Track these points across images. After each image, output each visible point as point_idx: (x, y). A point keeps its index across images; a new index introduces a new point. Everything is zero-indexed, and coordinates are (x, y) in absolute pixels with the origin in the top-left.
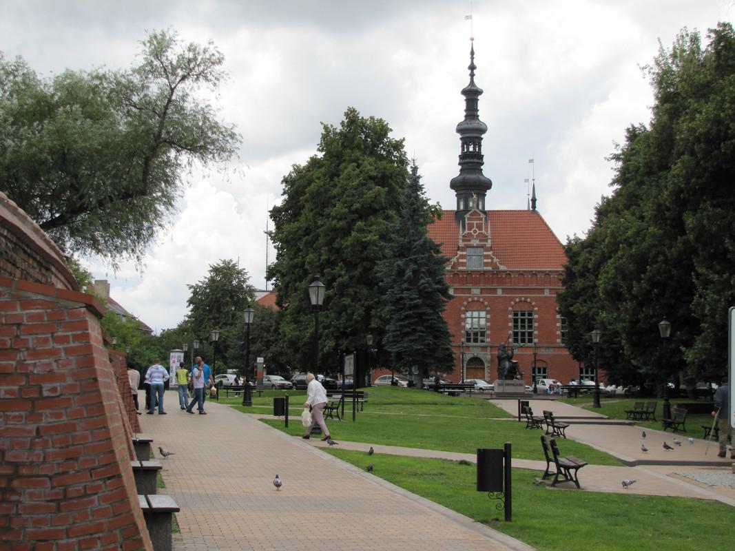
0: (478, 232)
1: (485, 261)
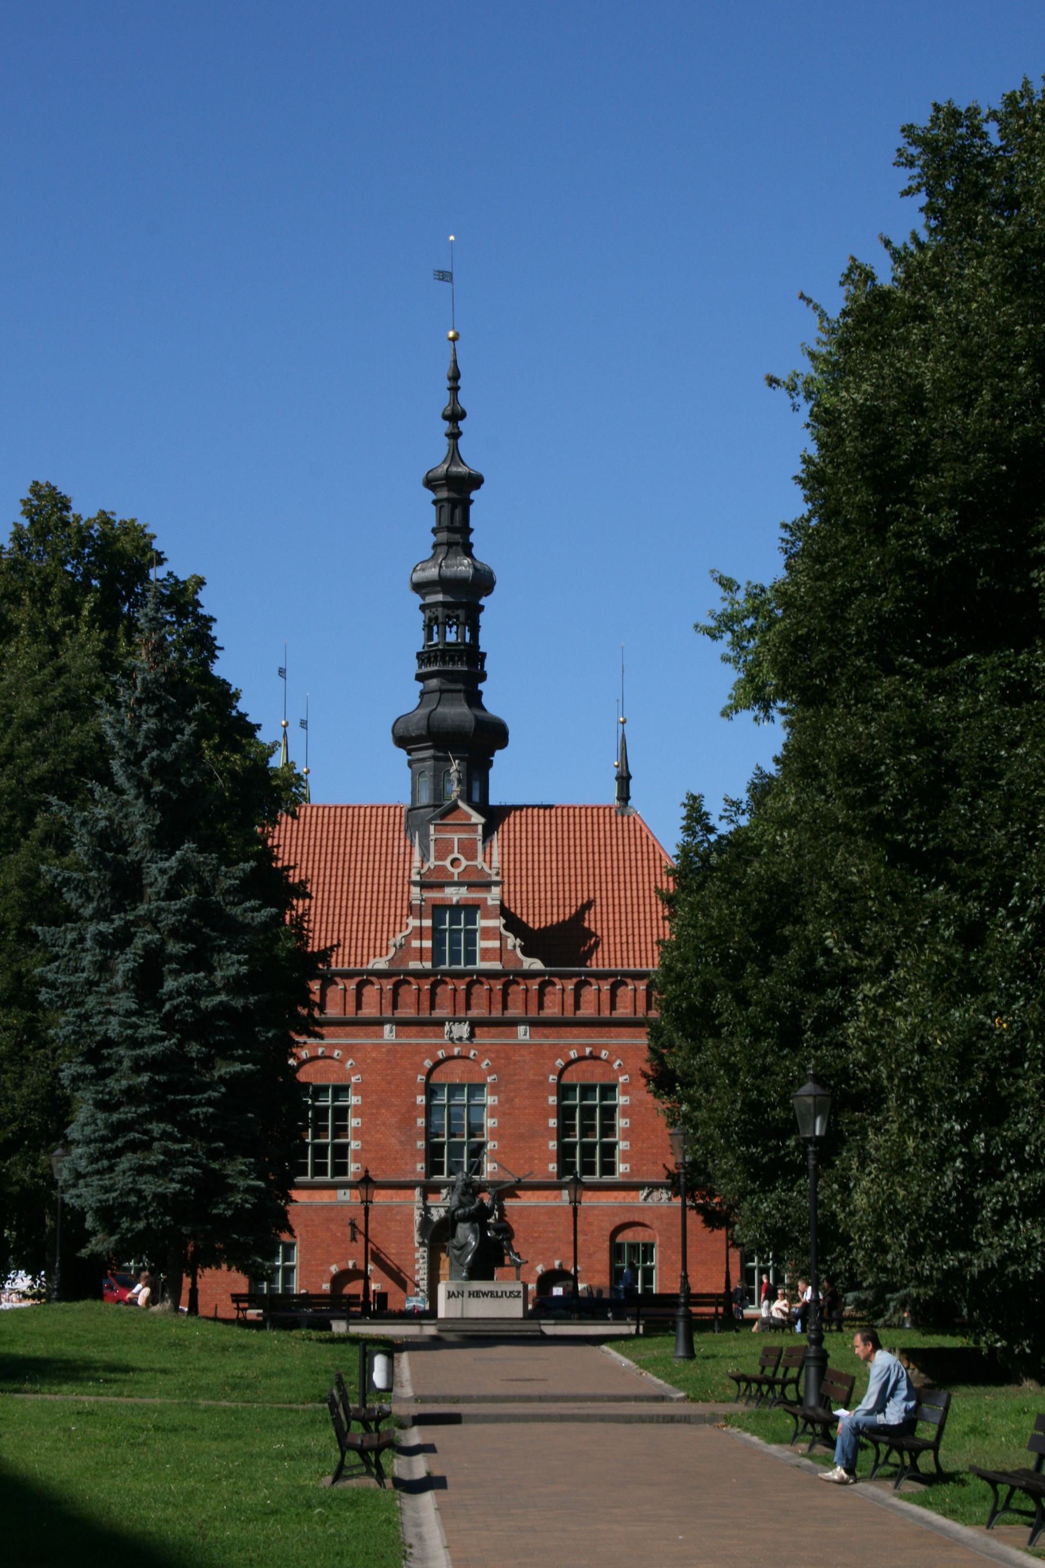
0: (464, 863)
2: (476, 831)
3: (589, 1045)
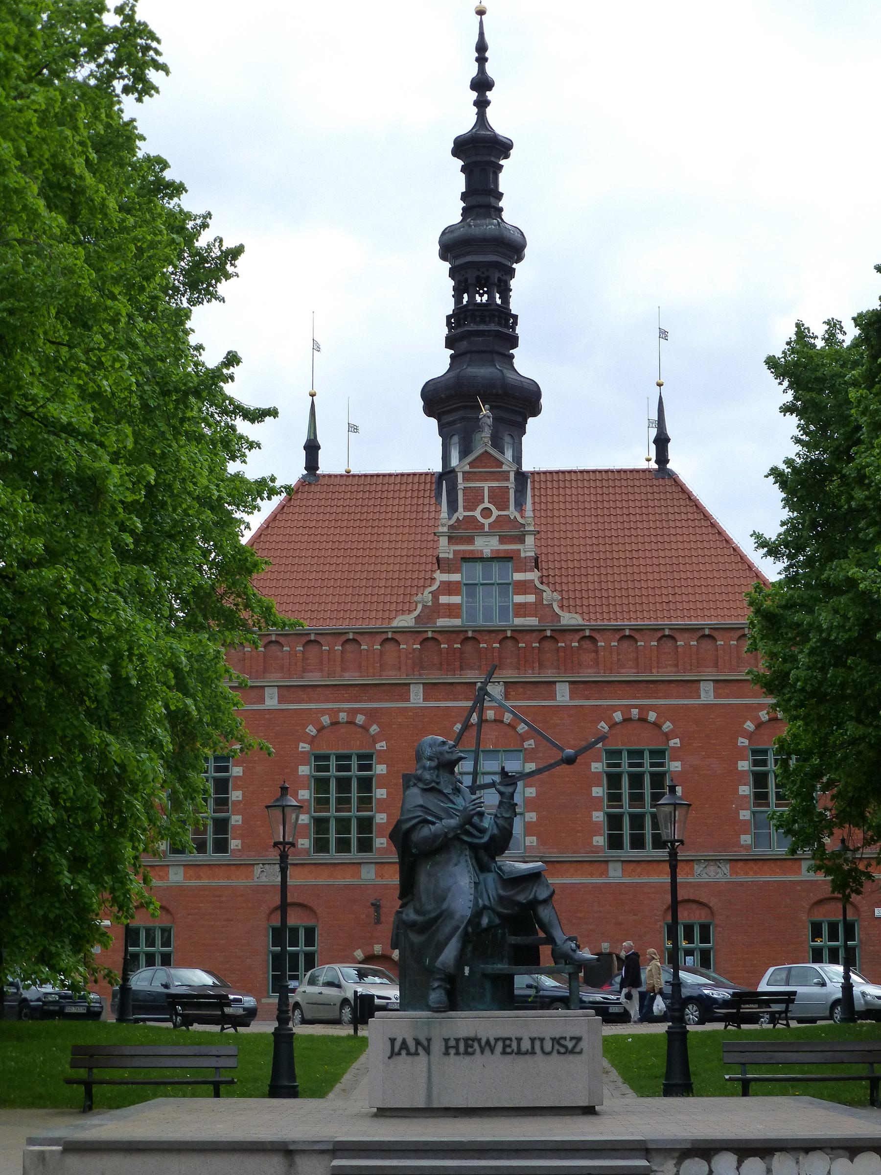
0: (496, 513)
1: (519, 599)
2: (508, 480)
3: (635, 706)
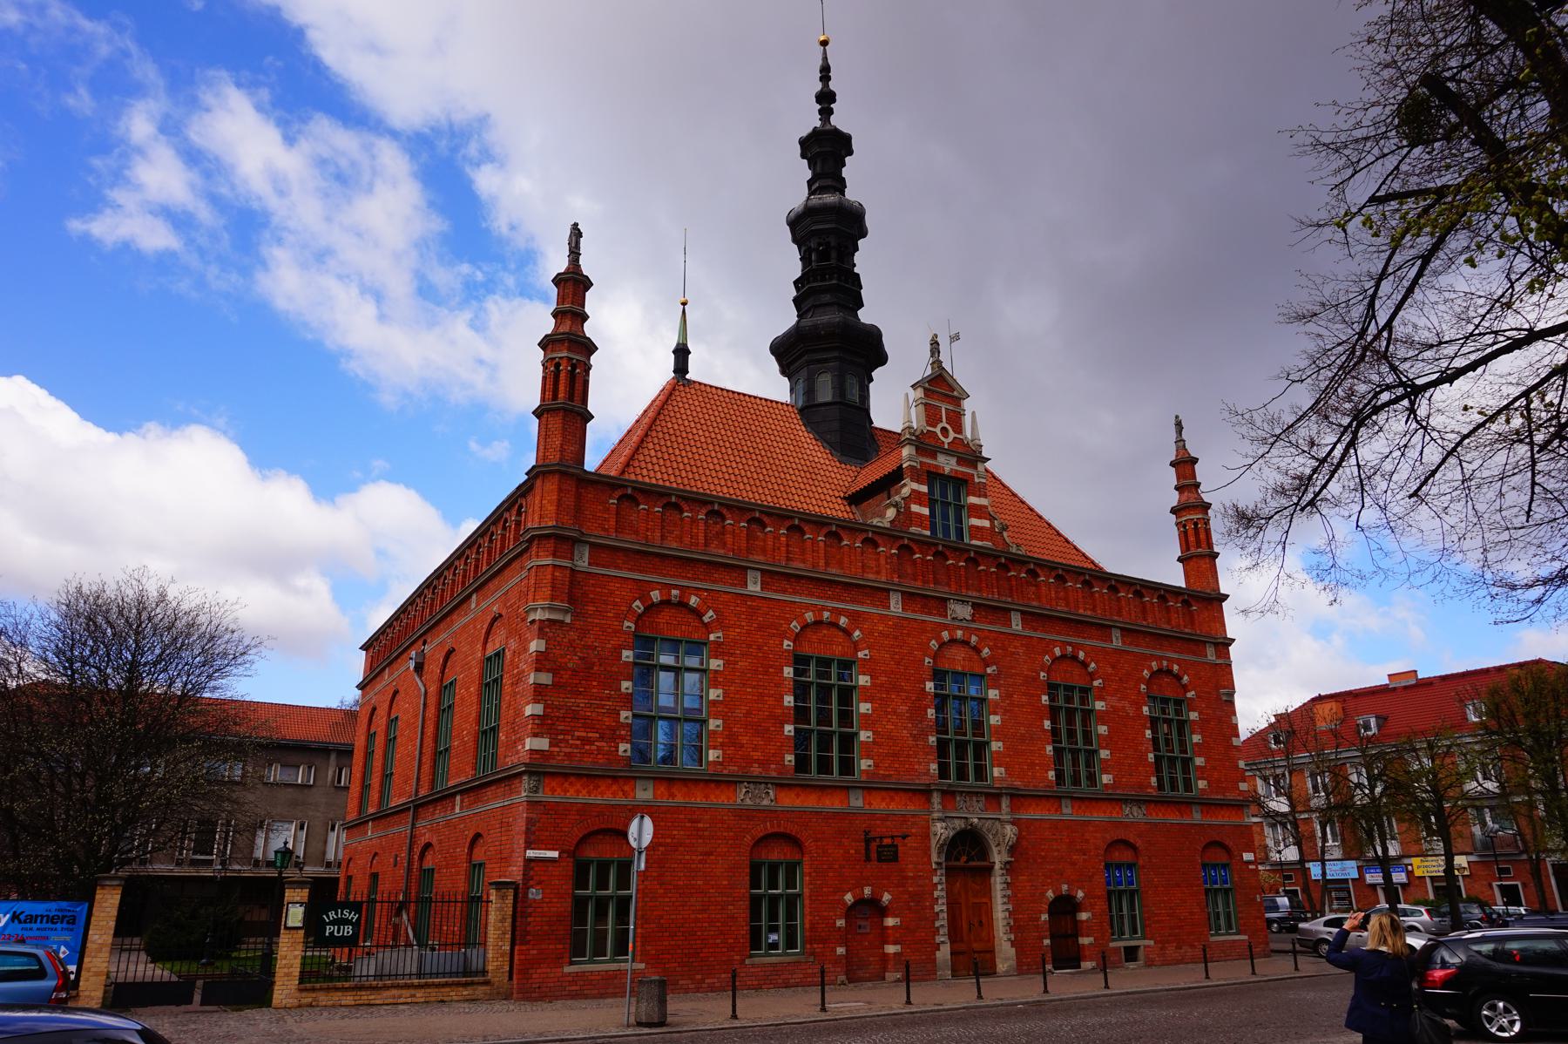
1: (975, 522)
